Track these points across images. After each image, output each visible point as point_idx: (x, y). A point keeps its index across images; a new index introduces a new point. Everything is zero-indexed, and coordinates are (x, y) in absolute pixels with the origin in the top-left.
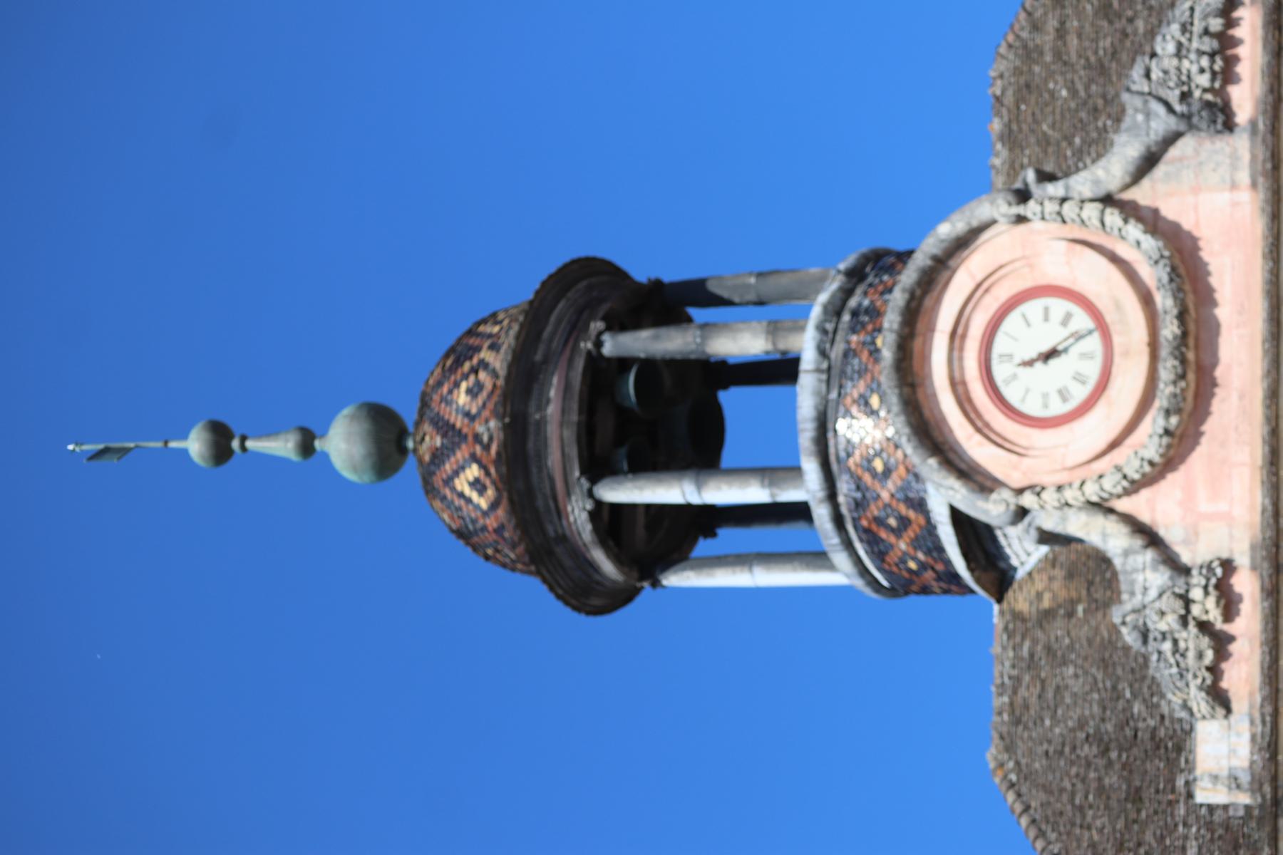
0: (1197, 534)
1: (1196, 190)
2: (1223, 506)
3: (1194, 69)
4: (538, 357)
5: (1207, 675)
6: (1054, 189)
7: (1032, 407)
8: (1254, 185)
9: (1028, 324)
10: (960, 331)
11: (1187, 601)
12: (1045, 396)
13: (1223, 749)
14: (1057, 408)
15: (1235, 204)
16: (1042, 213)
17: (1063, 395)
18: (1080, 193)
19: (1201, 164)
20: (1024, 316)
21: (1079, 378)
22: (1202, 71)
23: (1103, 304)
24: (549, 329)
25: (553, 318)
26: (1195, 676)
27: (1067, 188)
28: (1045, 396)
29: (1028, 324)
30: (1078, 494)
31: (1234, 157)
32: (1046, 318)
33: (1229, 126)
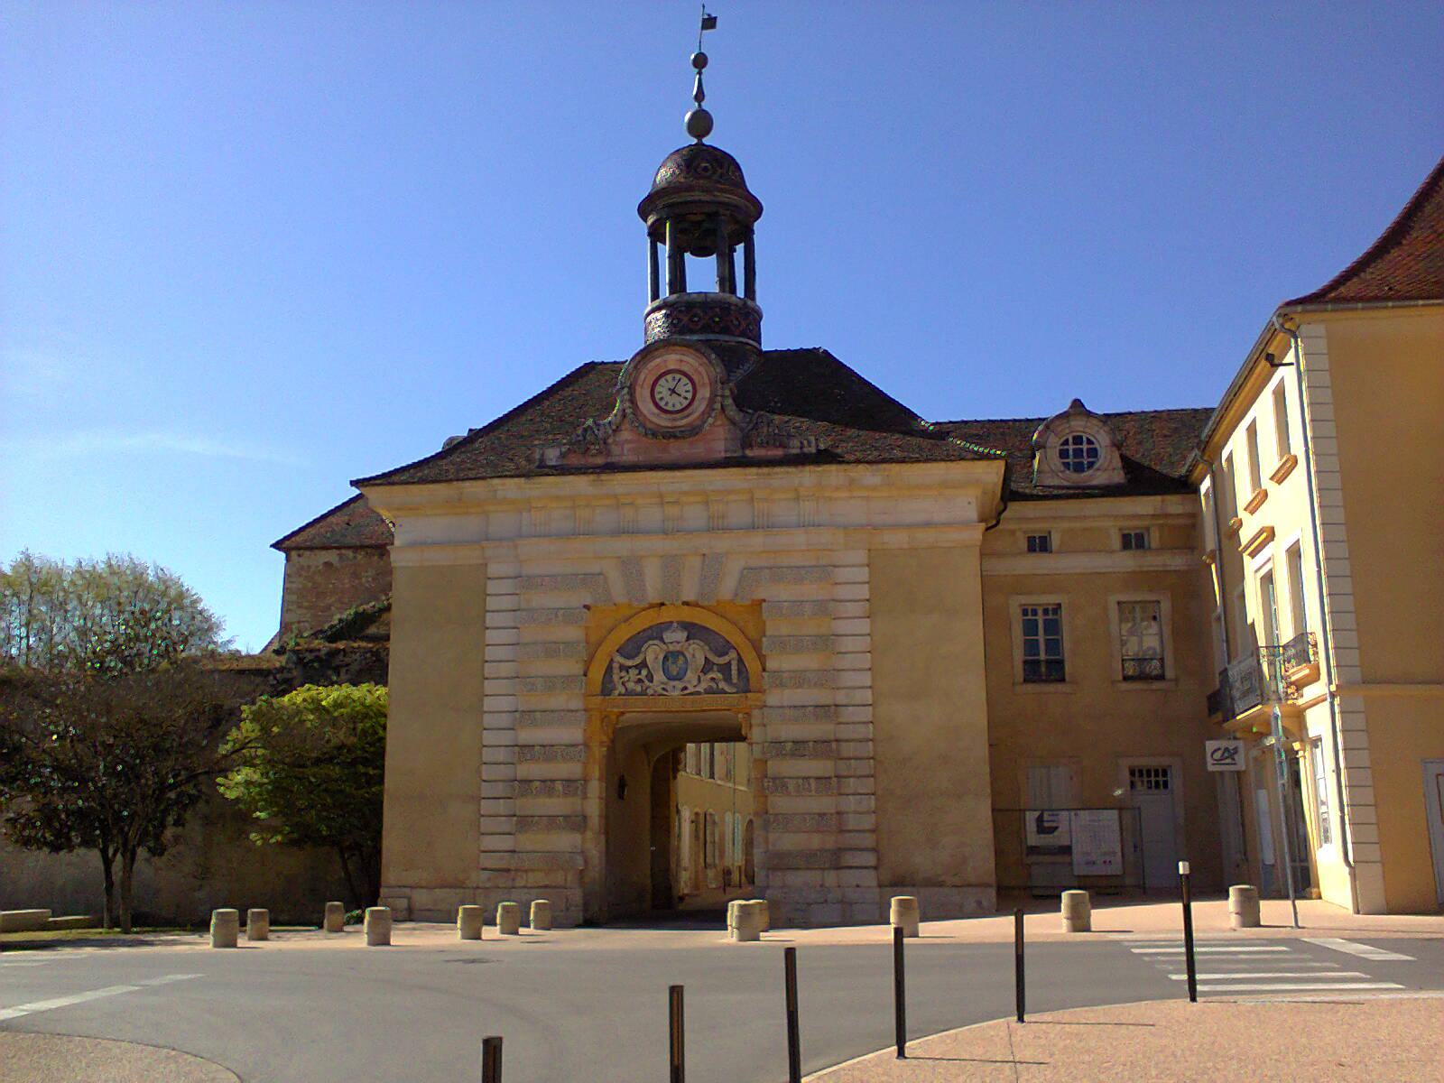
1: (726, 439)
2: (625, 452)
4: (716, 193)
6: (727, 393)
7: (658, 389)
8: (726, 458)
12: (660, 393)
13: (551, 457)
14: (658, 397)
15: (720, 452)
21: (667, 404)
27: (727, 396)
31: (735, 452)
32: (687, 391)
33: (743, 449)
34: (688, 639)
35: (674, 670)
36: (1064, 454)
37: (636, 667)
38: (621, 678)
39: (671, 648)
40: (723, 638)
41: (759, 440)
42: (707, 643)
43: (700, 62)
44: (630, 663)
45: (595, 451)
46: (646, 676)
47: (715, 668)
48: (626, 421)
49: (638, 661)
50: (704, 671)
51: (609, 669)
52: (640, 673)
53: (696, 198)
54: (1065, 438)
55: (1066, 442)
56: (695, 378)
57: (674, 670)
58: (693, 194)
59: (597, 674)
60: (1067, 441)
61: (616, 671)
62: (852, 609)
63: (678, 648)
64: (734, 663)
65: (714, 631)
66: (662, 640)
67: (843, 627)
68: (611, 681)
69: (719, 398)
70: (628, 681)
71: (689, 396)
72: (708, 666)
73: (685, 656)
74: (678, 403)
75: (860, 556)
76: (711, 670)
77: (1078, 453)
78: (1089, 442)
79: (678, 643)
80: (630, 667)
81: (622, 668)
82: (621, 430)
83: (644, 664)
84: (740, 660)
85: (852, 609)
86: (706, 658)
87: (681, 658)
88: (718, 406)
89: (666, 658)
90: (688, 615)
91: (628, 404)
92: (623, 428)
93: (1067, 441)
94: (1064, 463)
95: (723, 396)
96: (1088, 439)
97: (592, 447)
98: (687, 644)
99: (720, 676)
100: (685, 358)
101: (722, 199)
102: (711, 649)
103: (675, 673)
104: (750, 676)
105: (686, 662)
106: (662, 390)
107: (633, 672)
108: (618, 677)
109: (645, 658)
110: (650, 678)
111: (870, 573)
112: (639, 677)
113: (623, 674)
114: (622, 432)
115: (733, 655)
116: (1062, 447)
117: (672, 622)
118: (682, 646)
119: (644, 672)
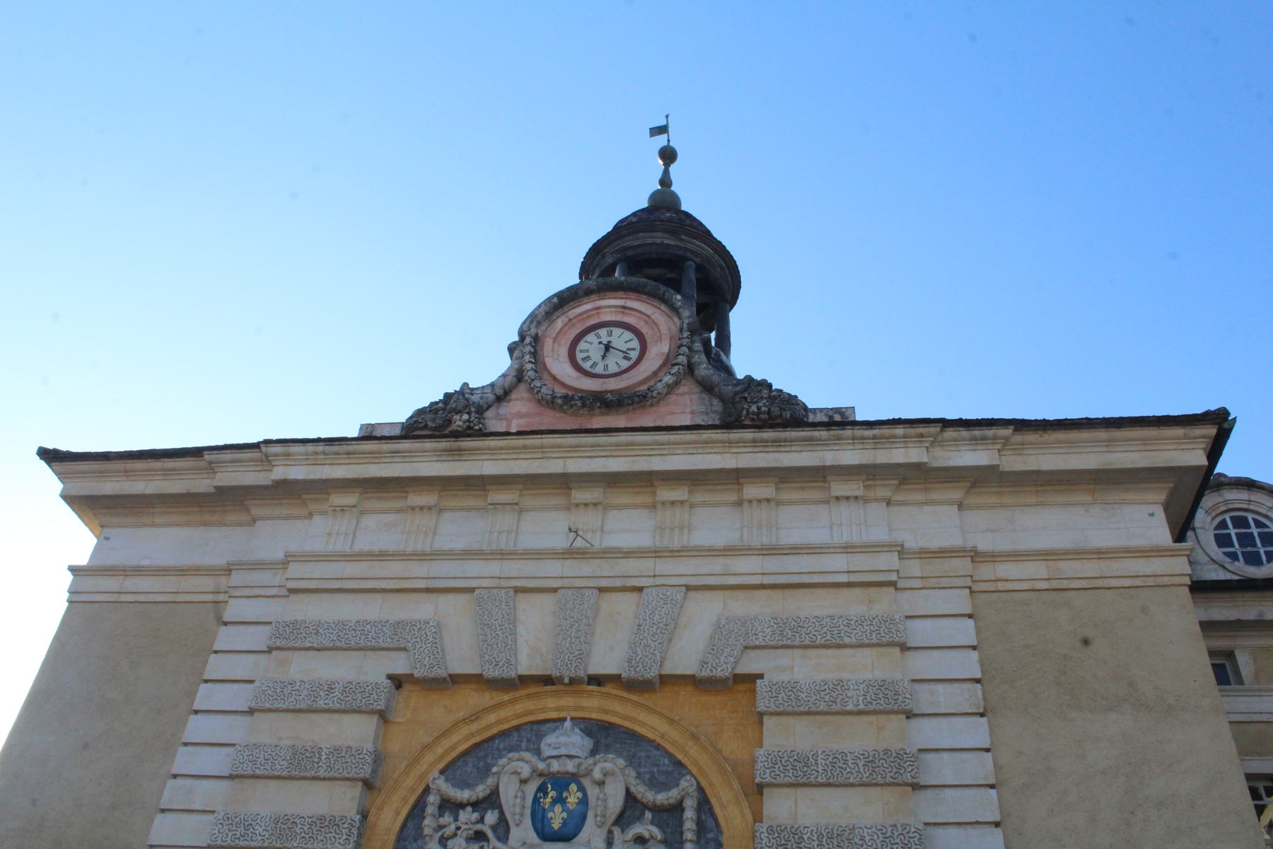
0: (501, 419)
3: (760, 404)
4: (683, 237)
5: (423, 424)
7: (582, 345)
9: (626, 342)
10: (627, 311)
11: (459, 412)
14: (579, 356)
16: (683, 338)
17: (586, 359)
18: (694, 357)
19: (707, 414)
20: (632, 340)
22: (759, 408)
23: (633, 372)
24: (699, 243)
25: (703, 245)
26: (423, 419)
28: (587, 351)
29: (626, 342)
30: (527, 361)
34: (593, 752)
35: (557, 818)
36: (1223, 541)
37: (476, 805)
38: (441, 827)
39: (556, 766)
40: (670, 755)
41: (754, 408)
42: (632, 761)
43: (668, 155)
44: (465, 795)
45: (461, 423)
46: (494, 828)
47: (648, 815)
48: (522, 387)
49: (481, 791)
50: (622, 820)
51: (418, 809)
52: (481, 820)
53: (659, 241)
54: (1219, 519)
55: (1223, 525)
56: (645, 330)
57: (557, 818)
58: (654, 234)
59: (389, 819)
60: (1224, 522)
61: (430, 810)
62: (946, 698)
63: (570, 766)
64: (690, 804)
65: (651, 742)
66: (538, 752)
67: (926, 733)
68: (419, 828)
69: (684, 349)
70: (455, 835)
71: (634, 355)
72: (632, 807)
73: (581, 788)
74: (615, 363)
75: (959, 601)
76: (640, 818)
77: (1246, 540)
78: (1259, 524)
79: (570, 757)
80: (462, 806)
81: (450, 806)
82: (510, 401)
83: (491, 800)
84: (704, 804)
85: (946, 698)
86: (628, 791)
87: (573, 787)
88: (682, 359)
89: (542, 789)
90: (594, 705)
91: (527, 358)
92: (513, 396)
93: (1224, 522)
94: (1225, 553)
95: (690, 349)
96: (1256, 521)
97: (457, 417)
98: (591, 761)
99: (655, 830)
100: (629, 303)
101: (690, 246)
102: (639, 775)
103: (556, 825)
104: (724, 839)
105: (584, 801)
106: (591, 347)
107: (466, 816)
108: (434, 825)
109: (497, 787)
110: (502, 828)
111: (977, 628)
112: (479, 827)
113: (447, 818)
114: (512, 403)
115: (686, 784)
116: (1217, 532)
117: (564, 719)
118: (579, 765)
119: (491, 817)
